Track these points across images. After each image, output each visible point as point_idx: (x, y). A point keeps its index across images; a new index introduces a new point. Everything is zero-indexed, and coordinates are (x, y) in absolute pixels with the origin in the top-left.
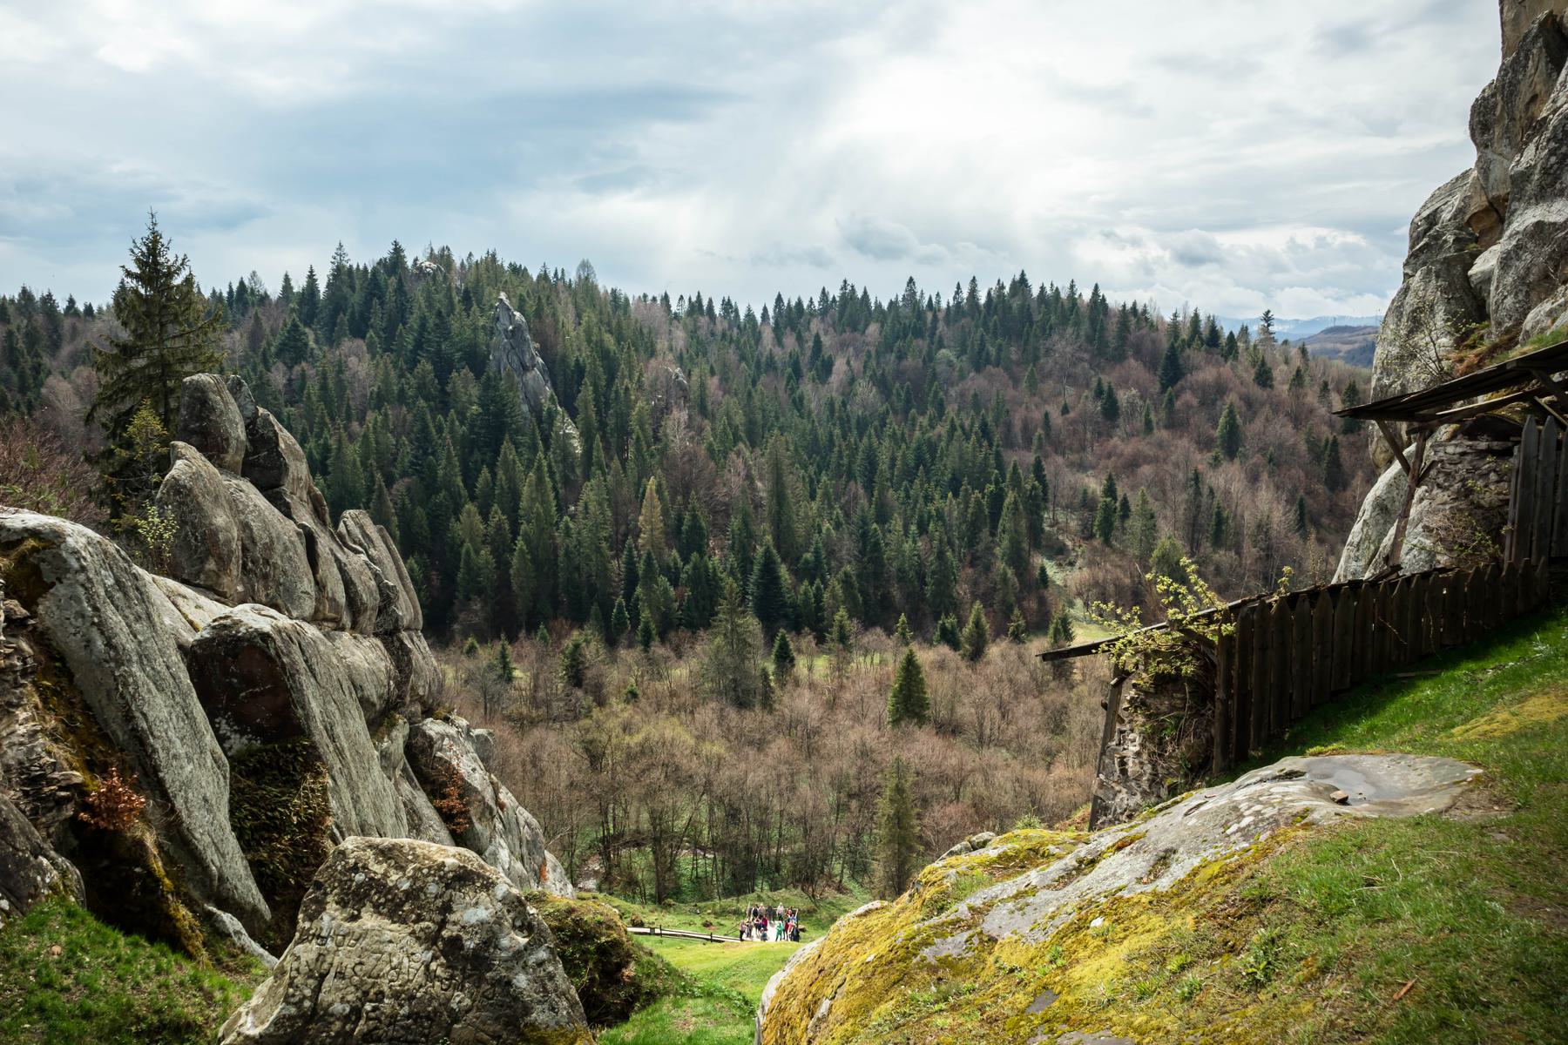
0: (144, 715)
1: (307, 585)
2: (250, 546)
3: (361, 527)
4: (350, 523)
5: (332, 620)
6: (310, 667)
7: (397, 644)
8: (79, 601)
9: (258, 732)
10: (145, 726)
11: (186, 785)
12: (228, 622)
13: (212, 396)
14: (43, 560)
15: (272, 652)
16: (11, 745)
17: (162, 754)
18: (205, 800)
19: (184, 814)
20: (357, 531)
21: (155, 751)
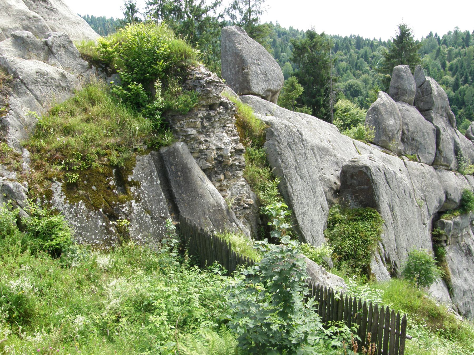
0: (291, 186)
1: (432, 149)
2: (406, 132)
6: (388, 182)
8: (275, 146)
10: (291, 191)
11: (304, 214)
13: (402, 73)
15: (369, 174)
16: (235, 188)
18: (312, 221)
19: (300, 223)
21: (293, 199)
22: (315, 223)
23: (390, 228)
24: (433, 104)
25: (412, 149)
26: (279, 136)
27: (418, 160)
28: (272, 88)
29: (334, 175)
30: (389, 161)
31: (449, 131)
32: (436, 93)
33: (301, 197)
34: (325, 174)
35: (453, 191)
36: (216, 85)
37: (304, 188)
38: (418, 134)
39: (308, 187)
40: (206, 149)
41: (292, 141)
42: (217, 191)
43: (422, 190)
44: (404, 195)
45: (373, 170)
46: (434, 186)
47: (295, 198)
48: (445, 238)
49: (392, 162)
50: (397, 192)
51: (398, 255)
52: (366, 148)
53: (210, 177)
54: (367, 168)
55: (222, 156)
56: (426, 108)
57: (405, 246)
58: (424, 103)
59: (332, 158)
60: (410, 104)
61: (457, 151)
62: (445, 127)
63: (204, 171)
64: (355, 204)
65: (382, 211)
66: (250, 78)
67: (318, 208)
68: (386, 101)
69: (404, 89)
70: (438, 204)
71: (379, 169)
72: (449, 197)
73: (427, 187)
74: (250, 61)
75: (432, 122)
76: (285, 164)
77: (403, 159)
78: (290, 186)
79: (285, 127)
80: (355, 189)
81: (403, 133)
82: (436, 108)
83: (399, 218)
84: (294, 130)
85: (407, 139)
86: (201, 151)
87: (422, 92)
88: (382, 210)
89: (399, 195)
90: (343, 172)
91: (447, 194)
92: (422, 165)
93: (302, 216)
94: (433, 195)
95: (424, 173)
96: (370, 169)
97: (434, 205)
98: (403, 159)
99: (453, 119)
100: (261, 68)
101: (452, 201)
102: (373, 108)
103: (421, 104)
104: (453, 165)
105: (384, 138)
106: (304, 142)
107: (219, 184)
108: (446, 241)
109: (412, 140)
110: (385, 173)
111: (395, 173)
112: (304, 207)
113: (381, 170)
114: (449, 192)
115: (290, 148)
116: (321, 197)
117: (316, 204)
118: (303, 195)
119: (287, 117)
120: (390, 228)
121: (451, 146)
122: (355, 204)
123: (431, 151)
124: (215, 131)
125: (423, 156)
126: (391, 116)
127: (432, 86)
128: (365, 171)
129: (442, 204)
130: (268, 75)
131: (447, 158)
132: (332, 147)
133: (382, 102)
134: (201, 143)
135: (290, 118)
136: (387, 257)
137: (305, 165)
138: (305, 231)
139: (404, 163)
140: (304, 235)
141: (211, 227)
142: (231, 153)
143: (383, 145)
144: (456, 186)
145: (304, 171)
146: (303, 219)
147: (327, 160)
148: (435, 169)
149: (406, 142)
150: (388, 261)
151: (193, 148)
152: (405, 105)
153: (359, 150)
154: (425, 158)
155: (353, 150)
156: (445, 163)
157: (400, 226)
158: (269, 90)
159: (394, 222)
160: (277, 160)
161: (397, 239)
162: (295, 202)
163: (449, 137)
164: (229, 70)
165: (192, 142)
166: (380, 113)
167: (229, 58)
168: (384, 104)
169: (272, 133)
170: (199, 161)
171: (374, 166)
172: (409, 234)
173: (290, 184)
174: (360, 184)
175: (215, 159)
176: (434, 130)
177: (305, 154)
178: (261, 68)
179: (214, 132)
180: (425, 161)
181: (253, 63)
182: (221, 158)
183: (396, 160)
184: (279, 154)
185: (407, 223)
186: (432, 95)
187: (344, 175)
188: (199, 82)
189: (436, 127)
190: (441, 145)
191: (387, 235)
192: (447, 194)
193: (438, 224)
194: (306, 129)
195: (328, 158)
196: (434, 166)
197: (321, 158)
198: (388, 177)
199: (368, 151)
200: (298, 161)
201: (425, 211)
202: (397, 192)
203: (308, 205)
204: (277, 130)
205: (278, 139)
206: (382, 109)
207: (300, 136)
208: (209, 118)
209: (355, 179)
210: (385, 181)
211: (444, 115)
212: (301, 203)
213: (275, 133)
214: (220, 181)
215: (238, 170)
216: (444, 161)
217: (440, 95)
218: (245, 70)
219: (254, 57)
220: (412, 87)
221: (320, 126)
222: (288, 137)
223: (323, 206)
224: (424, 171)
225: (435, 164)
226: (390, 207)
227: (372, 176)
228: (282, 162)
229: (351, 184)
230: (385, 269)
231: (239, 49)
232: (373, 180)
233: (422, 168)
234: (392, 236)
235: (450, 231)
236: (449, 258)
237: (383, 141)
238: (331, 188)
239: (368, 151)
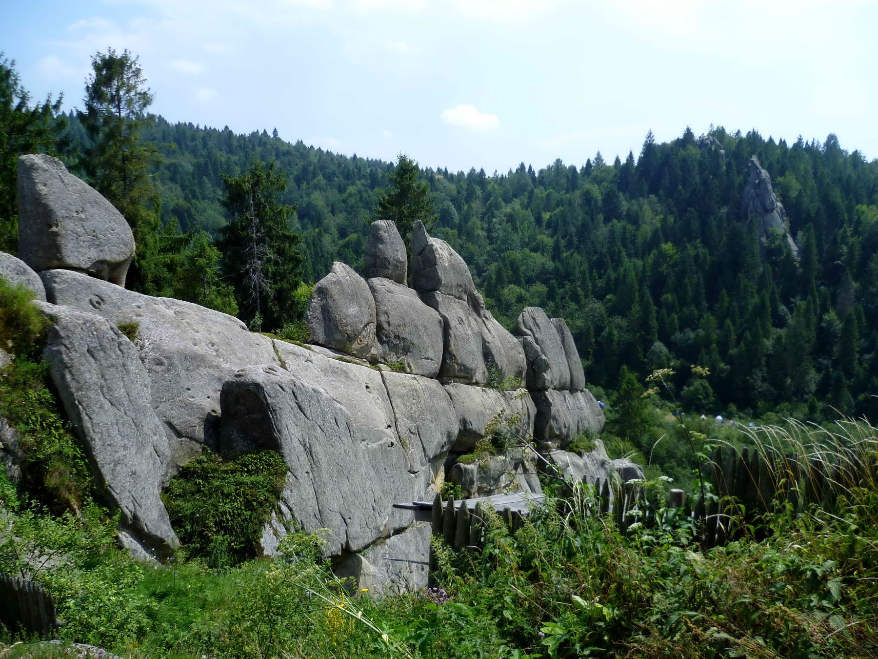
2: (385, 326)
3: (534, 319)
4: (526, 315)
5: (466, 378)
6: (300, 408)
7: (543, 398)
10: (89, 425)
11: (117, 463)
13: (382, 232)
19: (108, 478)
20: (531, 323)
21: (93, 439)
22: (139, 477)
23: (305, 481)
24: (439, 281)
26: (69, 337)
27: (409, 370)
28: (108, 258)
29: (213, 399)
30: (345, 372)
31: (473, 323)
32: (446, 264)
33: (109, 436)
34: (193, 397)
35: (476, 417)
37: (117, 420)
38: (407, 329)
39: (126, 418)
43: (412, 418)
44: (336, 427)
45: (267, 389)
46: (436, 411)
47: (97, 437)
49: (351, 375)
50: (320, 422)
52: (298, 353)
54: (257, 386)
56: (430, 287)
57: (336, 507)
58: (423, 279)
59: (211, 371)
60: (399, 281)
61: (487, 355)
62: (464, 318)
65: (286, 455)
66: (62, 241)
67: (147, 452)
68: (343, 277)
69: (386, 259)
70: (445, 439)
71: (281, 387)
73: (422, 413)
74: (60, 212)
75: (437, 309)
76: (78, 382)
77: (380, 370)
78: (87, 418)
79: (85, 323)
81: (379, 328)
82: (447, 287)
83: (324, 465)
84: (103, 328)
85: (386, 337)
88: (286, 450)
89: (323, 427)
91: (464, 422)
93: (112, 466)
94: (432, 425)
95: (416, 390)
96: (262, 388)
97: (436, 440)
98: (380, 370)
99: (479, 304)
100: (85, 224)
101: (478, 436)
102: (319, 288)
104: (480, 374)
106: (122, 347)
109: (395, 338)
110: (294, 393)
112: (116, 452)
114: (468, 420)
115: (93, 356)
117: (141, 446)
118: (114, 432)
119: (134, 305)
120: (305, 481)
121: (475, 347)
122: (245, 443)
123: (430, 354)
125: (416, 364)
126: (351, 301)
129: (454, 438)
130: (99, 236)
131: (464, 365)
132: (214, 353)
133: (334, 279)
135: (139, 307)
137: (122, 385)
138: (118, 491)
139: (382, 375)
140: (116, 496)
143: (338, 347)
144: (481, 409)
145: (120, 392)
146: (114, 470)
147: (200, 375)
148: (443, 383)
149: (385, 342)
152: (386, 281)
153: (283, 357)
154: (421, 367)
156: (462, 374)
157: (325, 476)
158: (103, 262)
160: (63, 377)
161: (321, 498)
162: (97, 444)
163: (469, 332)
166: (331, 297)
167: (28, 208)
168: (338, 283)
169: (57, 332)
171: (272, 383)
172: (345, 488)
173: (87, 414)
176: (440, 322)
177: (124, 365)
178: (85, 224)
180: (420, 371)
181: (70, 218)
183: (362, 371)
184: (67, 367)
185: (342, 472)
189: (443, 317)
190: (452, 346)
191: (298, 494)
192: (464, 422)
193: (454, 472)
194: (168, 325)
195: (203, 371)
196: (445, 379)
197: (187, 370)
198: (300, 399)
199: (302, 358)
200: (107, 377)
201: (415, 453)
202: (320, 422)
203: (125, 448)
204: (65, 328)
205: (67, 342)
206: (334, 290)
207: (114, 337)
210: (294, 405)
211: (465, 297)
212: (109, 445)
213: (62, 334)
217: (453, 266)
218: (54, 229)
219: (73, 208)
220: (399, 255)
221: (204, 319)
222: (88, 339)
223: (158, 449)
224: (418, 387)
225: (443, 375)
226: (305, 446)
227: (266, 399)
228: (74, 379)
231: (43, 193)
232: (268, 404)
233: (415, 384)
234: (308, 492)
235: (472, 482)
237: (338, 341)
239: (302, 358)
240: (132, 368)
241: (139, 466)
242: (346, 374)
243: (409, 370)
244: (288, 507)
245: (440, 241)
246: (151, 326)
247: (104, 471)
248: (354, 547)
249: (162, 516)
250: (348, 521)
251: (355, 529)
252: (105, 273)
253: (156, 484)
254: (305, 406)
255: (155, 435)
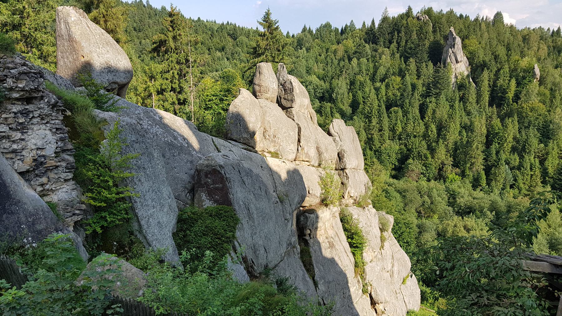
2: (268, 129)
9: (216, 201)
12: (210, 159)
14: (105, 129)
15: (223, 172)
17: (138, 204)
18: (159, 222)
19: (145, 227)
21: (136, 202)
23: (246, 226)
25: (274, 146)
28: (118, 81)
32: (298, 92)
36: (32, 76)
40: (23, 149)
41: (134, 139)
42: (37, 196)
47: (138, 200)
48: (309, 232)
49: (253, 159)
51: (255, 252)
53: (27, 180)
54: (221, 166)
55: (44, 156)
57: (261, 243)
63: (22, 174)
64: (211, 203)
67: (165, 210)
72: (310, 192)
75: (293, 120)
80: (209, 188)
86: (14, 151)
87: (285, 90)
88: (237, 208)
90: (197, 170)
92: (284, 162)
103: (284, 102)
105: (245, 135)
107: (42, 189)
108: (310, 235)
111: (251, 170)
113: (236, 168)
116: (170, 198)
117: (162, 206)
118: (147, 197)
119: (136, 112)
122: (211, 203)
124: (35, 129)
127: (294, 84)
128: (219, 169)
132: (186, 145)
134: (14, 142)
136: (244, 255)
141: (30, 239)
142: (55, 153)
150: (245, 260)
151: (4, 148)
152: (266, 101)
155: (212, 148)
158: (115, 83)
159: (250, 219)
161: (254, 236)
164: (65, 57)
165: (4, 141)
170: (14, 162)
174: (214, 183)
175: (35, 160)
179: (33, 129)
182: (43, 159)
186: (294, 93)
187: (199, 174)
188: (9, 72)
189: (298, 125)
208: (25, 113)
209: (209, 178)
214: (42, 185)
215: (66, 172)
216: (306, 157)
226: (245, 204)
229: (205, 183)
230: (241, 268)
232: (227, 178)
236: (313, 252)
238: (185, 188)
240: (155, 155)
241: (158, 220)
242: (251, 159)
243: (280, 157)
244: (238, 242)
245: (293, 77)
246: (149, 127)
247: (143, 223)
248: (271, 266)
249: (174, 251)
250: (267, 250)
251: (271, 255)
252: (116, 91)
253: (171, 230)
254: (245, 179)
255: (170, 198)
